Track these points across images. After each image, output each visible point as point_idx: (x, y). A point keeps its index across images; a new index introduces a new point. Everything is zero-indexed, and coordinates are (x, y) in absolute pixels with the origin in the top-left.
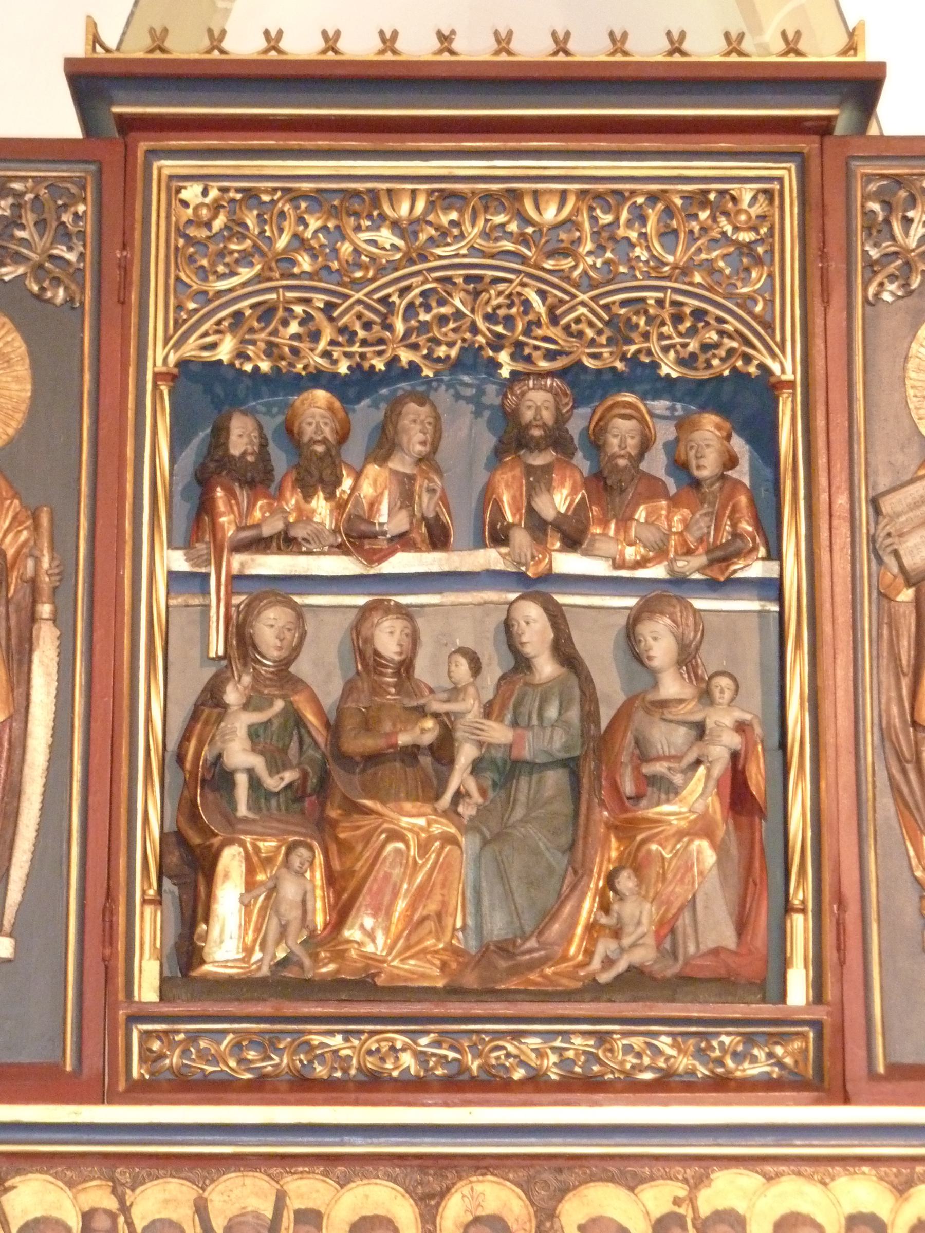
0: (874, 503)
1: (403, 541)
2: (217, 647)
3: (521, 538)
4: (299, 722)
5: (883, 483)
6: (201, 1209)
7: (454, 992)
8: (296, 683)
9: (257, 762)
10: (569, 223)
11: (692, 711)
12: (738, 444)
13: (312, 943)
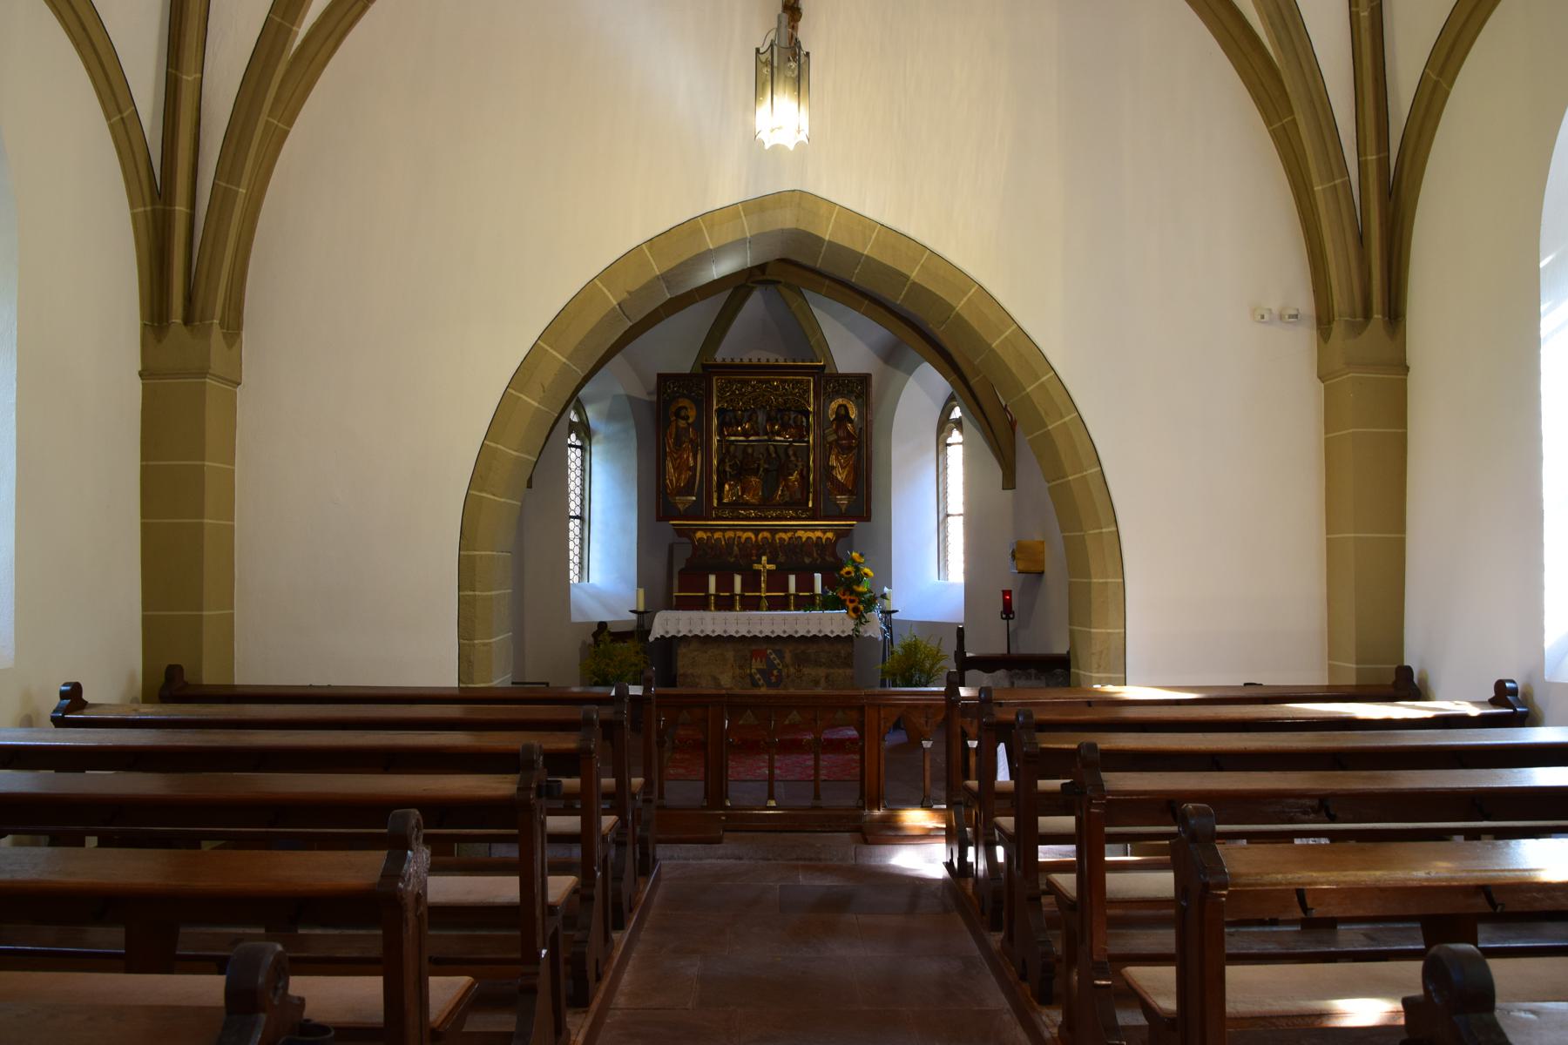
0: (824, 431)
1: (752, 435)
2: (724, 451)
3: (770, 435)
4: (736, 463)
5: (825, 427)
6: (724, 536)
7: (759, 505)
8: (735, 457)
9: (730, 470)
10: (778, 386)
11: (795, 462)
12: (804, 419)
13: (739, 497)
